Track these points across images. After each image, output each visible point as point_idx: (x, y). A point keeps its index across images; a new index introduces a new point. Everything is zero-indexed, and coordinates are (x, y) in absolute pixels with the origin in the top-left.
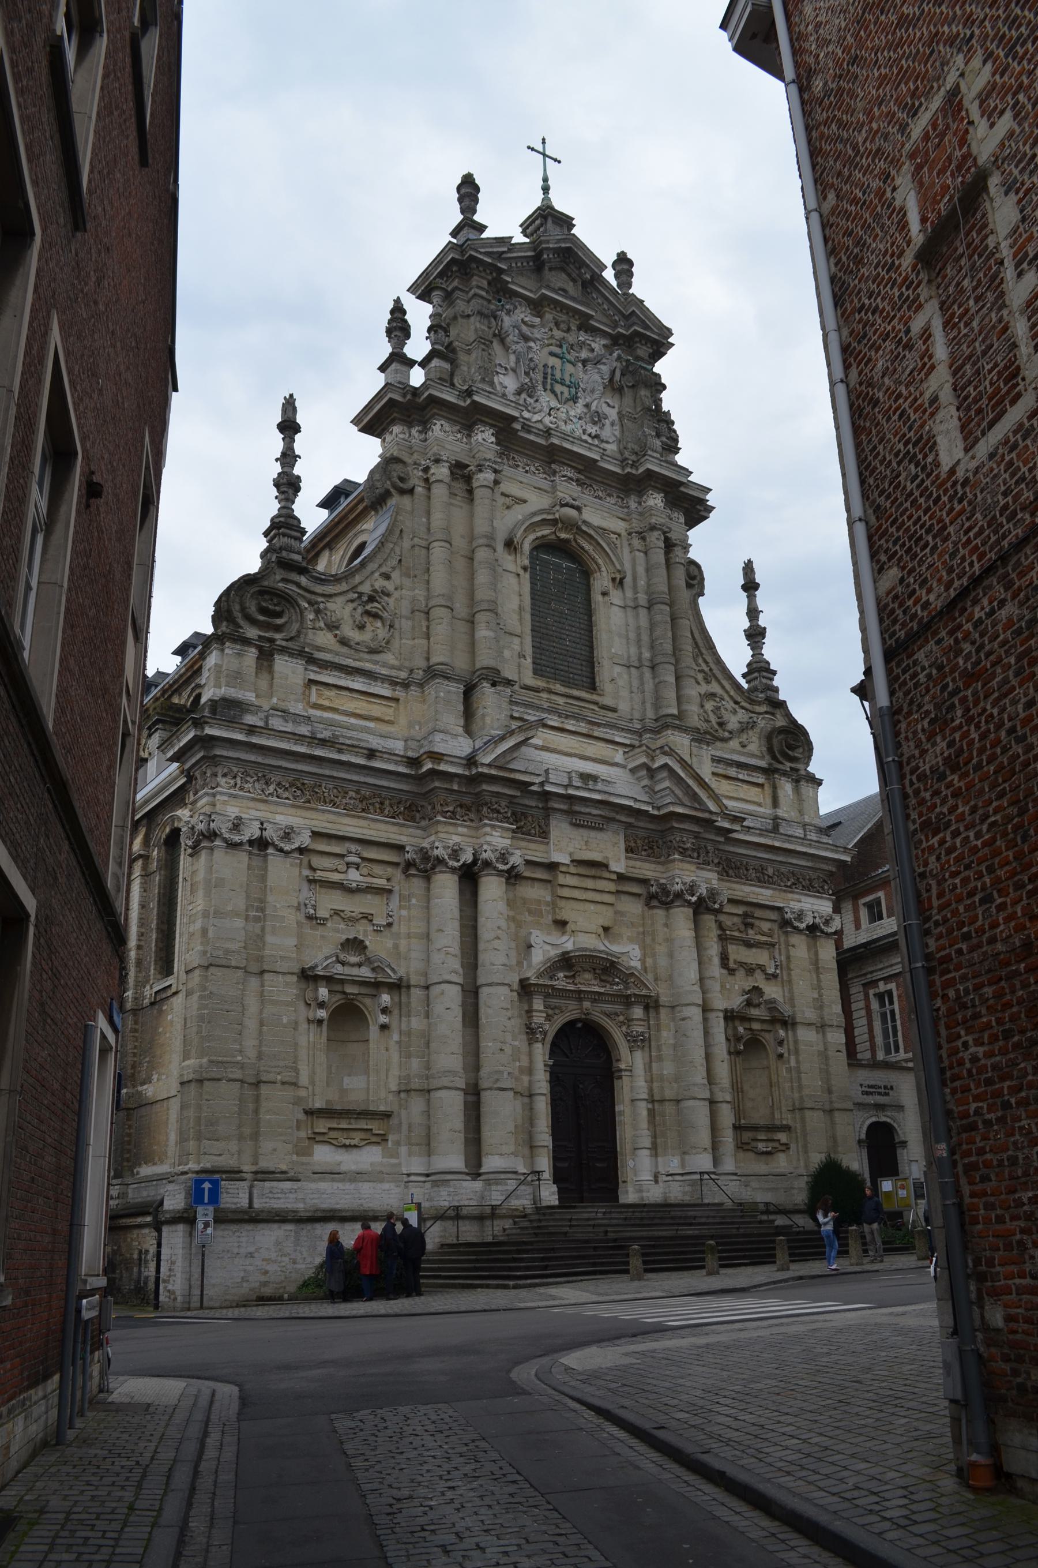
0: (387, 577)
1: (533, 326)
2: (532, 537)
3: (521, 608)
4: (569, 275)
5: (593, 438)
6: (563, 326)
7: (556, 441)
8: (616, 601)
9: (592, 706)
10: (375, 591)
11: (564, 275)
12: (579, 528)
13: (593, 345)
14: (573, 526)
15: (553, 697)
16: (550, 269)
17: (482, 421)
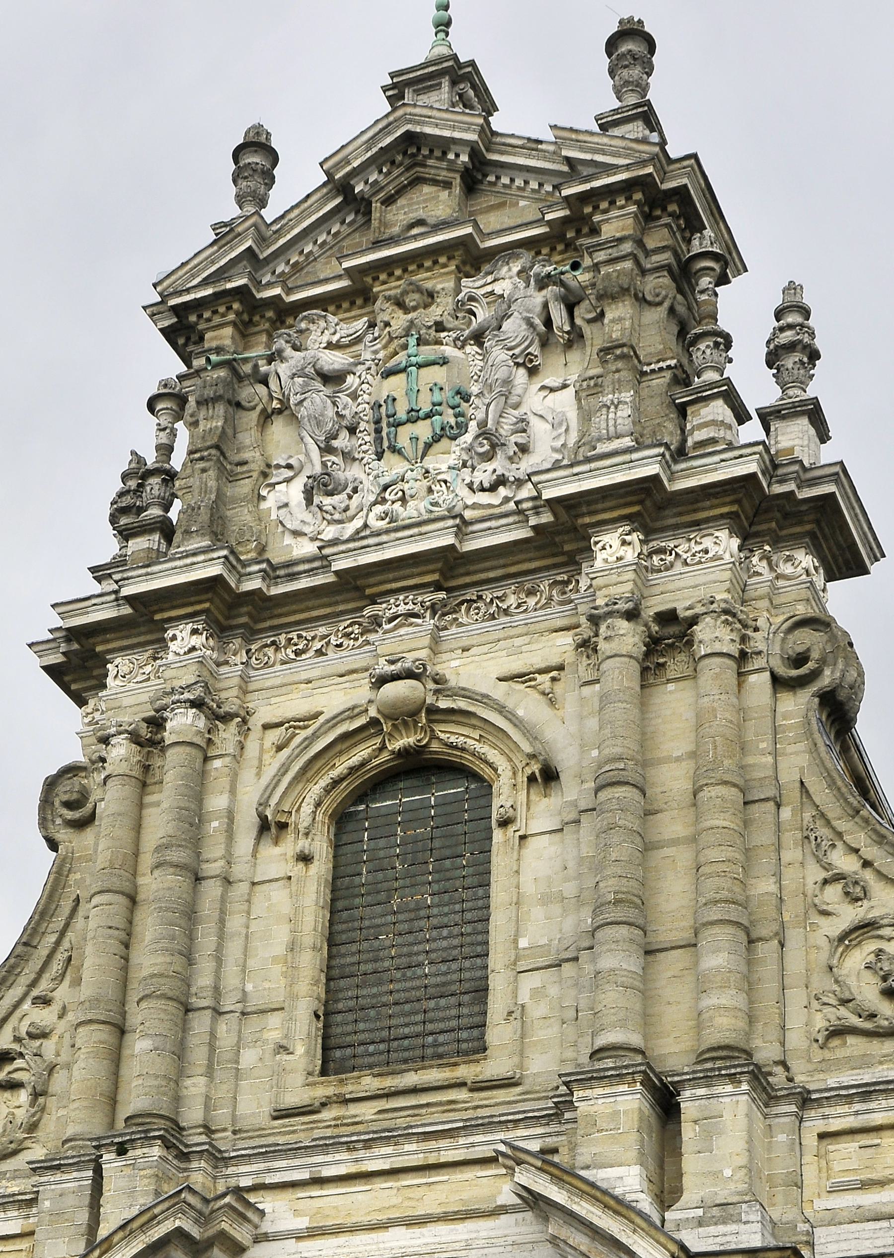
0: (44, 1001)
1: (358, 340)
2: (316, 789)
3: (292, 947)
4: (435, 182)
5: (493, 488)
6: (411, 300)
7: (340, 565)
8: (534, 828)
9: (452, 1095)
10: (17, 1039)
11: (427, 189)
12: (432, 711)
13: (498, 288)
14: (414, 714)
15: (353, 1109)
16: (389, 201)
17: (170, 620)
